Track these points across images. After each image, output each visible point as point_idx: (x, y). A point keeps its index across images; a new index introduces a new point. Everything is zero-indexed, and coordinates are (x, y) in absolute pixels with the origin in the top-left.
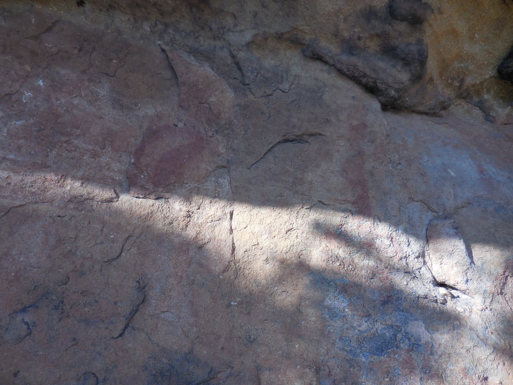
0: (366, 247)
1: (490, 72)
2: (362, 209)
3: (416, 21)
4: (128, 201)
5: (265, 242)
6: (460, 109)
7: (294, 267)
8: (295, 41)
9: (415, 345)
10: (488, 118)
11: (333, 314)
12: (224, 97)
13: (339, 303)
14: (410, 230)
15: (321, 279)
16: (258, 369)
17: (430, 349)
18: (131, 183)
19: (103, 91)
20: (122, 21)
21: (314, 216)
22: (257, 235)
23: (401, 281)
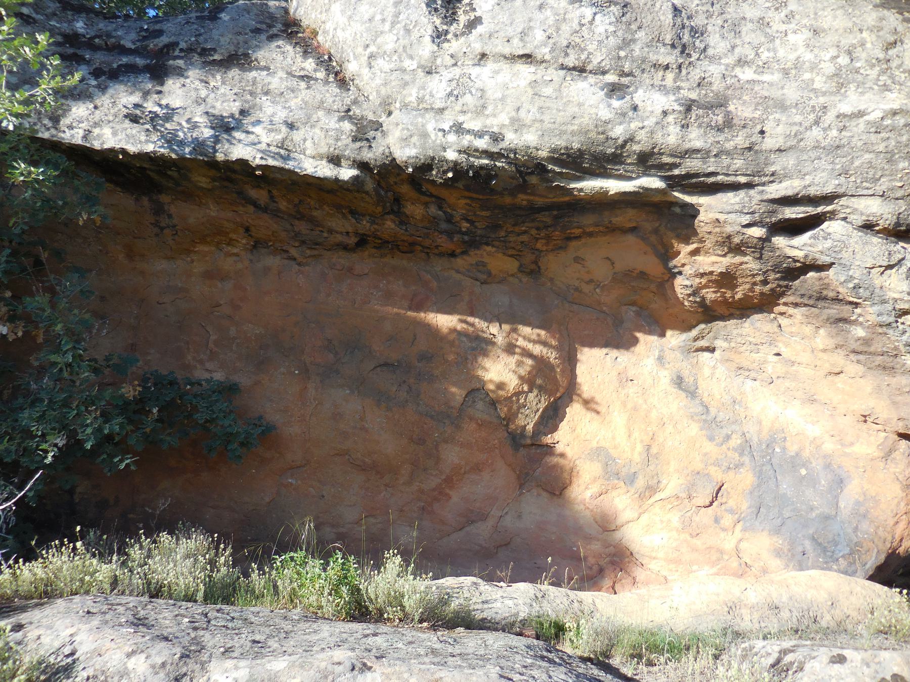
0: (472, 325)
1: (516, 270)
2: (472, 314)
3: (484, 266)
4: (409, 313)
5: (446, 324)
6: (511, 279)
7: (453, 330)
8: (453, 269)
9: (482, 349)
10: (521, 281)
11: (462, 342)
12: (434, 284)
13: (464, 339)
14: (486, 320)
15: (460, 333)
16: (443, 355)
17: (486, 350)
18: (410, 309)
19: (401, 282)
20: (405, 262)
21: (458, 317)
22: (445, 321)
23: (480, 334)
